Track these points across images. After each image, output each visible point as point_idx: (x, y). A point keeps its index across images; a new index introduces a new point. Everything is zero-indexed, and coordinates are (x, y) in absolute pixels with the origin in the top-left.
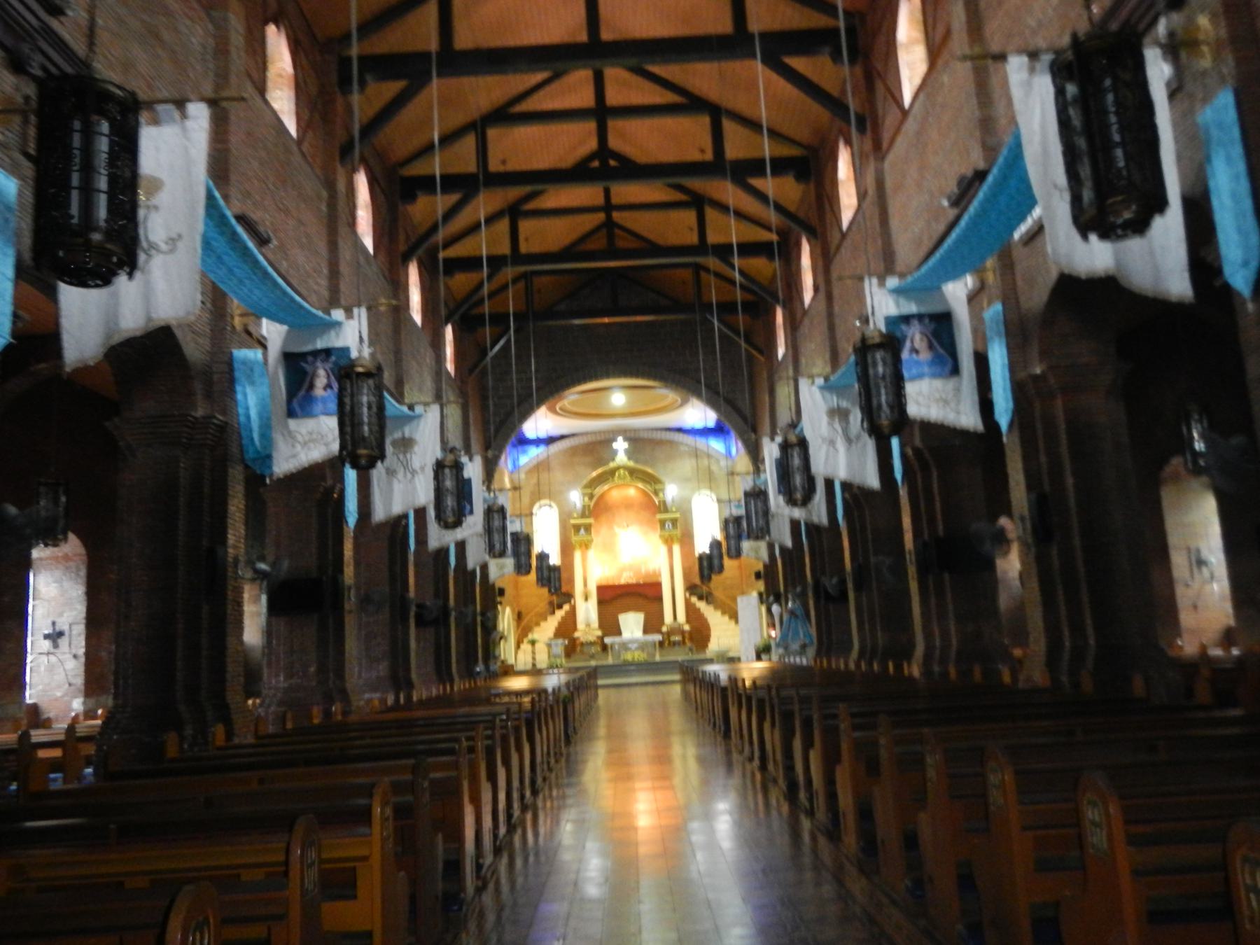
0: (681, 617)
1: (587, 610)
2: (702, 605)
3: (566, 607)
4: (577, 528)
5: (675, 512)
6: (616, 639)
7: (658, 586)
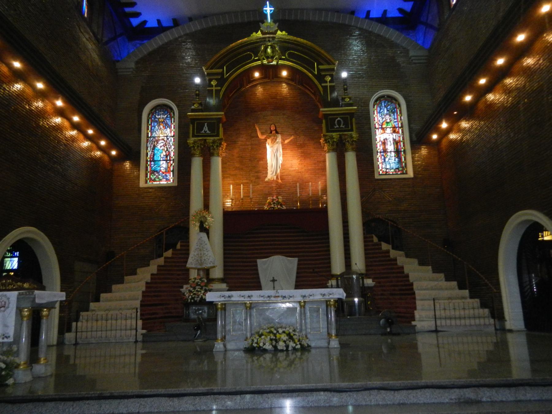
4: (198, 123)
5: (351, 105)
6: (237, 296)
7: (324, 212)
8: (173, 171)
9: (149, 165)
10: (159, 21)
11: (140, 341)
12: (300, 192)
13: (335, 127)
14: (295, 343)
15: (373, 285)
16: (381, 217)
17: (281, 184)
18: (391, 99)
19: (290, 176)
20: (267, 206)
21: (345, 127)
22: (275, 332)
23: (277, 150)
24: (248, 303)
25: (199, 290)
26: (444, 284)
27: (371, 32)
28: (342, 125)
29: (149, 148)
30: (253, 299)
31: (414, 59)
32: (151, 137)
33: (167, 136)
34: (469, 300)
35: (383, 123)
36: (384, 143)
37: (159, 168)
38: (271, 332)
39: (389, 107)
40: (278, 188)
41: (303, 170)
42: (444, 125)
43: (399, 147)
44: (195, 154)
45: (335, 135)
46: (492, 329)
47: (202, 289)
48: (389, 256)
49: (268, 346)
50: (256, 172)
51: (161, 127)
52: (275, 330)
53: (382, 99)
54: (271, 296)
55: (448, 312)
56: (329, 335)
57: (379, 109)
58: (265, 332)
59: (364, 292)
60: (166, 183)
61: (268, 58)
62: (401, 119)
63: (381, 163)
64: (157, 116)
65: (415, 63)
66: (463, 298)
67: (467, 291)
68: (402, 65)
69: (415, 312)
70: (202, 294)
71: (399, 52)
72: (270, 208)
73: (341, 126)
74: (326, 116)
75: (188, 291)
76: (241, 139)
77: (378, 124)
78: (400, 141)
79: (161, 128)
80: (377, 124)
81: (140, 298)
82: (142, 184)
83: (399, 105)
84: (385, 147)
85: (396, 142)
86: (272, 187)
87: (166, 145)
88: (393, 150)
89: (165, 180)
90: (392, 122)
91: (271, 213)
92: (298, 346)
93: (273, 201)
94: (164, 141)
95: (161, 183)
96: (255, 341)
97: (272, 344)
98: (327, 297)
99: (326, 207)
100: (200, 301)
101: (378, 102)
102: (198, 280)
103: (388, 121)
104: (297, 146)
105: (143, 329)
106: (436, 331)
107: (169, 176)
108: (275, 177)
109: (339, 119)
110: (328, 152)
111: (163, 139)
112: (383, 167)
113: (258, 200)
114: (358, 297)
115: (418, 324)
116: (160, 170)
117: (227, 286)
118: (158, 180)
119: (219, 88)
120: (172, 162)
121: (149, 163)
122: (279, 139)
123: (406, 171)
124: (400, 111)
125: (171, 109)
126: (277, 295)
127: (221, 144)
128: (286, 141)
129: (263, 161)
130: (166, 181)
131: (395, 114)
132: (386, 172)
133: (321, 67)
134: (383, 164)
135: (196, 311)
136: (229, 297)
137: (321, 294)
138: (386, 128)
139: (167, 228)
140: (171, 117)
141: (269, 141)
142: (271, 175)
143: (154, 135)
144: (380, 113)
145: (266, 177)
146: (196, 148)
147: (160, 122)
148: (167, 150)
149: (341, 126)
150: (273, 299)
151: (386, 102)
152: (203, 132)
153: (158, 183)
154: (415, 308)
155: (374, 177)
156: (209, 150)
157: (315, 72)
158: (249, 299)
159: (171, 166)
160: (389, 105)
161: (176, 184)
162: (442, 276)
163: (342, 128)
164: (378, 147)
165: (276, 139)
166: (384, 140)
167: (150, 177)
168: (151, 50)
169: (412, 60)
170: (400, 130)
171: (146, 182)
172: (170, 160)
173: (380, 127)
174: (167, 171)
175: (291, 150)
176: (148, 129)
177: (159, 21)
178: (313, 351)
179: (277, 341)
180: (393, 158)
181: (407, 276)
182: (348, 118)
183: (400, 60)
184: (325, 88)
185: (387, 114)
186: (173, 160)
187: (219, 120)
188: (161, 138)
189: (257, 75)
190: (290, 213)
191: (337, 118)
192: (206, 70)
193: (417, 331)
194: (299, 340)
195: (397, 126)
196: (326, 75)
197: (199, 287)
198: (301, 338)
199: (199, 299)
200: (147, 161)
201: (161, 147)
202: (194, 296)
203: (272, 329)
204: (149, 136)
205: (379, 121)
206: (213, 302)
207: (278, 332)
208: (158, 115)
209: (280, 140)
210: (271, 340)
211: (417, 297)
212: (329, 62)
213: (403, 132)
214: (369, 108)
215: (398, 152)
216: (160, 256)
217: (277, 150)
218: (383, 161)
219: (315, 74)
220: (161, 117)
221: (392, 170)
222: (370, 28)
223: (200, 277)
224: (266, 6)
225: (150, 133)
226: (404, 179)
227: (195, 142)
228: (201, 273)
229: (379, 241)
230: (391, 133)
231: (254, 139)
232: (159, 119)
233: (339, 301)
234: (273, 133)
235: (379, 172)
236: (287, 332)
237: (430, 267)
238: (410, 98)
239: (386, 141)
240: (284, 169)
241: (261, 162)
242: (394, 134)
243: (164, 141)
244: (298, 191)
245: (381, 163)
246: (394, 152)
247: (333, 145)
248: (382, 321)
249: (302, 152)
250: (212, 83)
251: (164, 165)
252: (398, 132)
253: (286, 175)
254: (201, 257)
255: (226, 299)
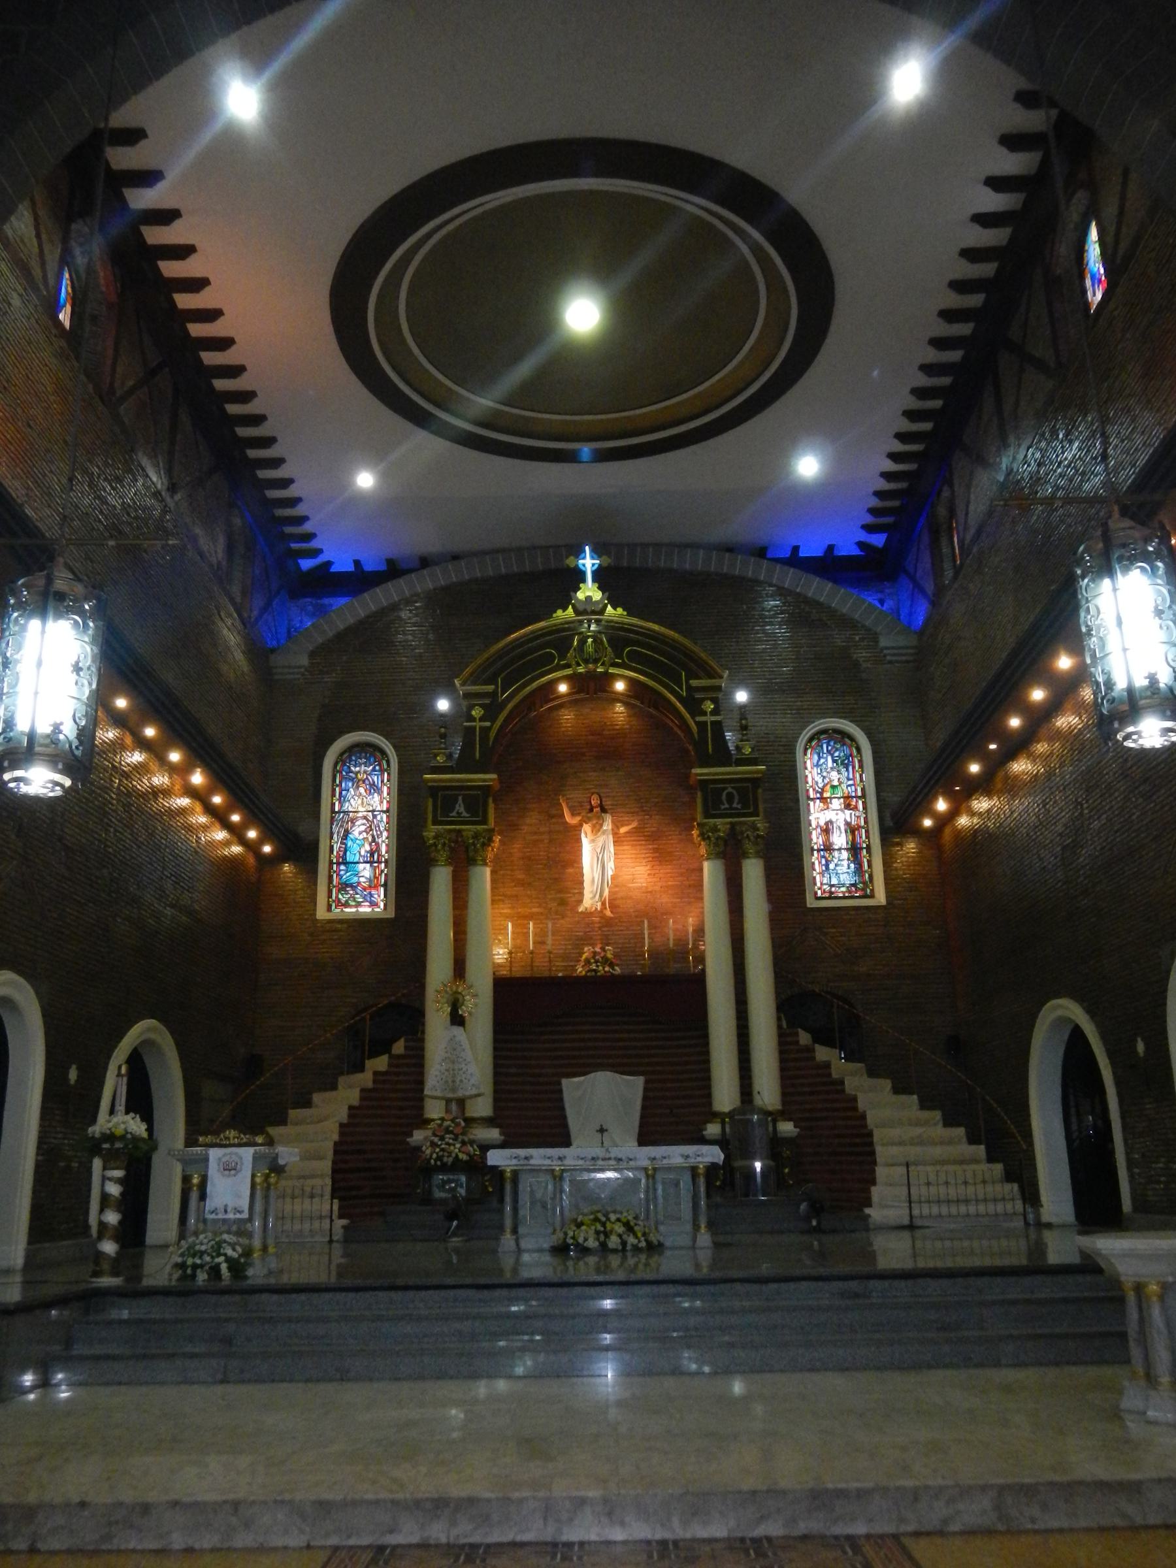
0: (767, 1091)
1: (454, 1047)
2: (822, 1053)
3: (399, 1047)
4: (444, 798)
6: (539, 1156)
7: (700, 980)
8: (385, 885)
9: (335, 872)
10: (357, 563)
11: (337, 1241)
12: (649, 934)
13: (723, 807)
14: (636, 1237)
15: (796, 1134)
16: (817, 990)
17: (611, 918)
18: (842, 737)
19: (629, 901)
20: (583, 966)
21: (743, 808)
22: (603, 1219)
23: (603, 848)
24: (558, 1169)
25: (451, 1141)
26: (940, 1131)
27: (799, 594)
28: (736, 800)
29: (335, 836)
30: (566, 1162)
31: (889, 654)
32: (339, 812)
33: (373, 811)
34: (984, 1166)
35: (825, 786)
36: (827, 830)
37: (355, 879)
38: (596, 1220)
39: (837, 754)
40: (603, 927)
41: (657, 888)
42: (941, 805)
43: (858, 840)
44: (437, 861)
45: (722, 824)
46: (1019, 1223)
47: (455, 1139)
48: (830, 1075)
49: (592, 1243)
50: (560, 891)
51: (362, 790)
52: (604, 1215)
53: (822, 737)
54: (598, 1158)
55: (933, 1190)
56: (696, 1227)
57: (816, 757)
58: (587, 1219)
59: (775, 1148)
60: (369, 910)
61: (586, 662)
62: (861, 780)
63: (819, 873)
64: (353, 768)
65: (890, 662)
66: (976, 1161)
67: (982, 1147)
68: (864, 665)
69: (873, 1189)
70: (457, 1150)
71: (857, 638)
72: (589, 971)
73: (735, 805)
74: (704, 784)
75: (428, 1144)
76: (528, 821)
77: (814, 790)
78: (859, 827)
79: (360, 794)
80: (811, 790)
81: (330, 1154)
82: (321, 914)
83: (859, 750)
84: (828, 839)
85: (852, 830)
86: (593, 923)
87: (371, 830)
88: (845, 846)
89: (368, 904)
90: (844, 786)
91: (592, 983)
92: (643, 1244)
93: (594, 957)
94: (368, 820)
95: (361, 910)
96: (571, 1234)
97: (598, 1239)
98: (693, 1160)
99: (703, 971)
100: (453, 1163)
101: (813, 743)
102: (448, 1123)
103: (836, 783)
104: (644, 836)
105: (341, 1217)
106: (911, 1227)
107: (376, 896)
108: (599, 904)
109: (730, 790)
110: (707, 859)
111: (365, 818)
112: (825, 882)
113: (561, 951)
114: (761, 1160)
115: (875, 1214)
116: (359, 883)
117: (501, 1134)
118: (353, 903)
119: (488, 724)
120: (383, 865)
121: (335, 866)
122: (608, 825)
123: (872, 890)
124: (860, 762)
125: (383, 753)
126: (607, 1156)
127: (490, 840)
128: (623, 830)
129: (573, 867)
130: (370, 906)
131: (850, 768)
132: (831, 893)
133: (694, 683)
134: (823, 876)
135: (444, 1182)
136: (526, 1158)
137: (682, 1156)
138: (831, 798)
139: (374, 1009)
140: (382, 771)
141: (587, 828)
142: (590, 900)
143: (346, 807)
144: (817, 765)
145: (580, 901)
146: (440, 846)
147: (359, 780)
148: (374, 840)
149: (735, 805)
150: (600, 1162)
151: (832, 743)
152: (454, 814)
153: (354, 910)
154: (873, 1182)
155: (805, 903)
156: (467, 851)
157: (682, 690)
158: (560, 1163)
159: (380, 875)
160: (837, 750)
161: (391, 914)
162: (937, 1115)
163: (737, 809)
164: (815, 840)
165: (601, 825)
166: (827, 824)
167: (337, 897)
168: (342, 627)
169: (885, 656)
170: (860, 802)
171: (329, 909)
172: (379, 862)
173: (818, 795)
174: (373, 884)
175: (632, 845)
176: (333, 795)
177: (357, 563)
178: (668, 1253)
179: (607, 1234)
180: (845, 863)
181: (863, 1117)
182: (747, 791)
183: (861, 655)
184: (702, 726)
185: (832, 769)
186: (386, 862)
187: (486, 790)
188: (360, 815)
189: (563, 688)
190: (627, 981)
191: (725, 789)
192: (463, 684)
193: (871, 1226)
194: (644, 1234)
195: (853, 794)
196: (703, 700)
197: (452, 1136)
198: (647, 1230)
199: (451, 1159)
200: (331, 863)
201: (360, 833)
202: (441, 1153)
203: (600, 1215)
204: (337, 809)
205: (817, 783)
206: (498, 1166)
207: (608, 1219)
208: (355, 766)
209: (610, 827)
210: (597, 1233)
211: (880, 1159)
212: (712, 674)
213: (865, 808)
214: (795, 757)
215: (854, 850)
216: (362, 1069)
217: (603, 848)
218: (824, 868)
219: (682, 696)
220: (362, 769)
221: (843, 889)
222: (798, 585)
223: (451, 1117)
224: (583, 555)
225: (337, 803)
226: (867, 908)
227: (436, 837)
228: (454, 1107)
229: (816, 1040)
230: (841, 810)
231: (553, 820)
232: (356, 773)
233: (712, 1168)
234: (595, 812)
235: (816, 893)
236: (624, 1220)
237: (915, 1097)
238: (881, 736)
239: (830, 827)
240: (616, 886)
241: (570, 870)
242: (848, 812)
243: (368, 820)
244: (646, 932)
245: (819, 873)
246: (847, 849)
247: (716, 845)
248: (803, 1206)
249: (656, 850)
250: (473, 713)
251: (366, 871)
252: (856, 808)
253: (622, 898)
254: (454, 1076)
255: (522, 1162)
